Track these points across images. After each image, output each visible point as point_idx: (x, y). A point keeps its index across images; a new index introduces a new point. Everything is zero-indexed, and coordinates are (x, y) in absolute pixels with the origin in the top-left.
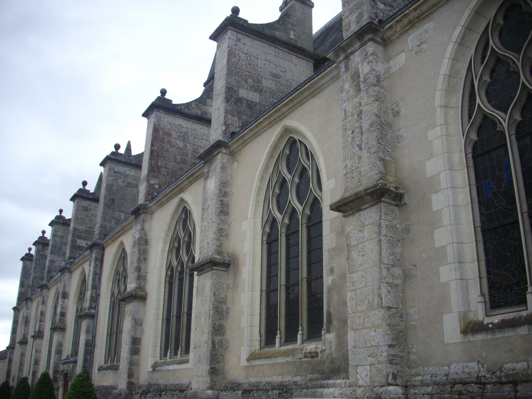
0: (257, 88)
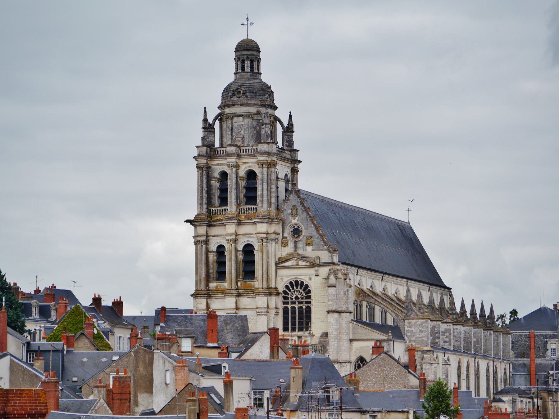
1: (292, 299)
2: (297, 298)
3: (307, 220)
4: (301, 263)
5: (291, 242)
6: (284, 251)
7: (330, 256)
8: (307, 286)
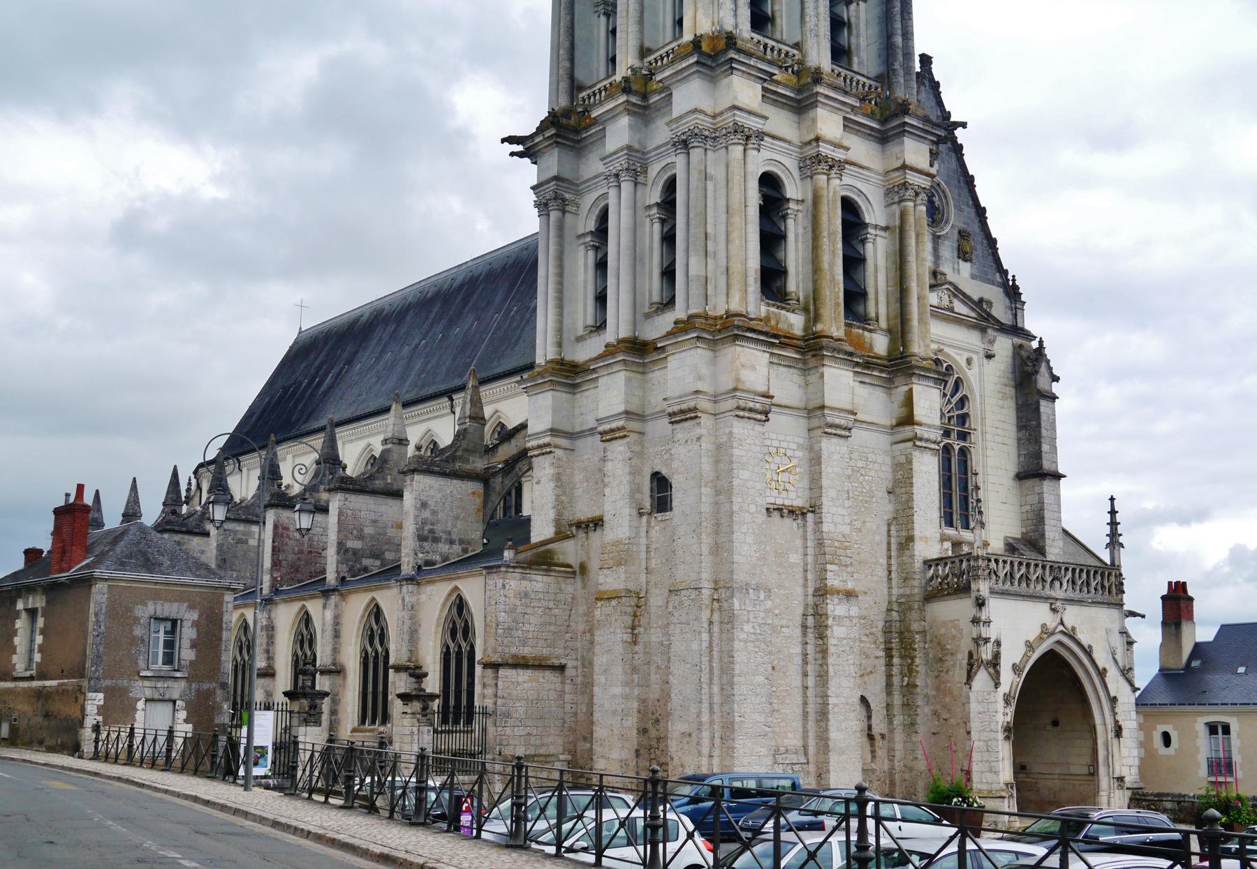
0: (361, 537)
3: (959, 182)
4: (960, 308)
8: (958, 384)
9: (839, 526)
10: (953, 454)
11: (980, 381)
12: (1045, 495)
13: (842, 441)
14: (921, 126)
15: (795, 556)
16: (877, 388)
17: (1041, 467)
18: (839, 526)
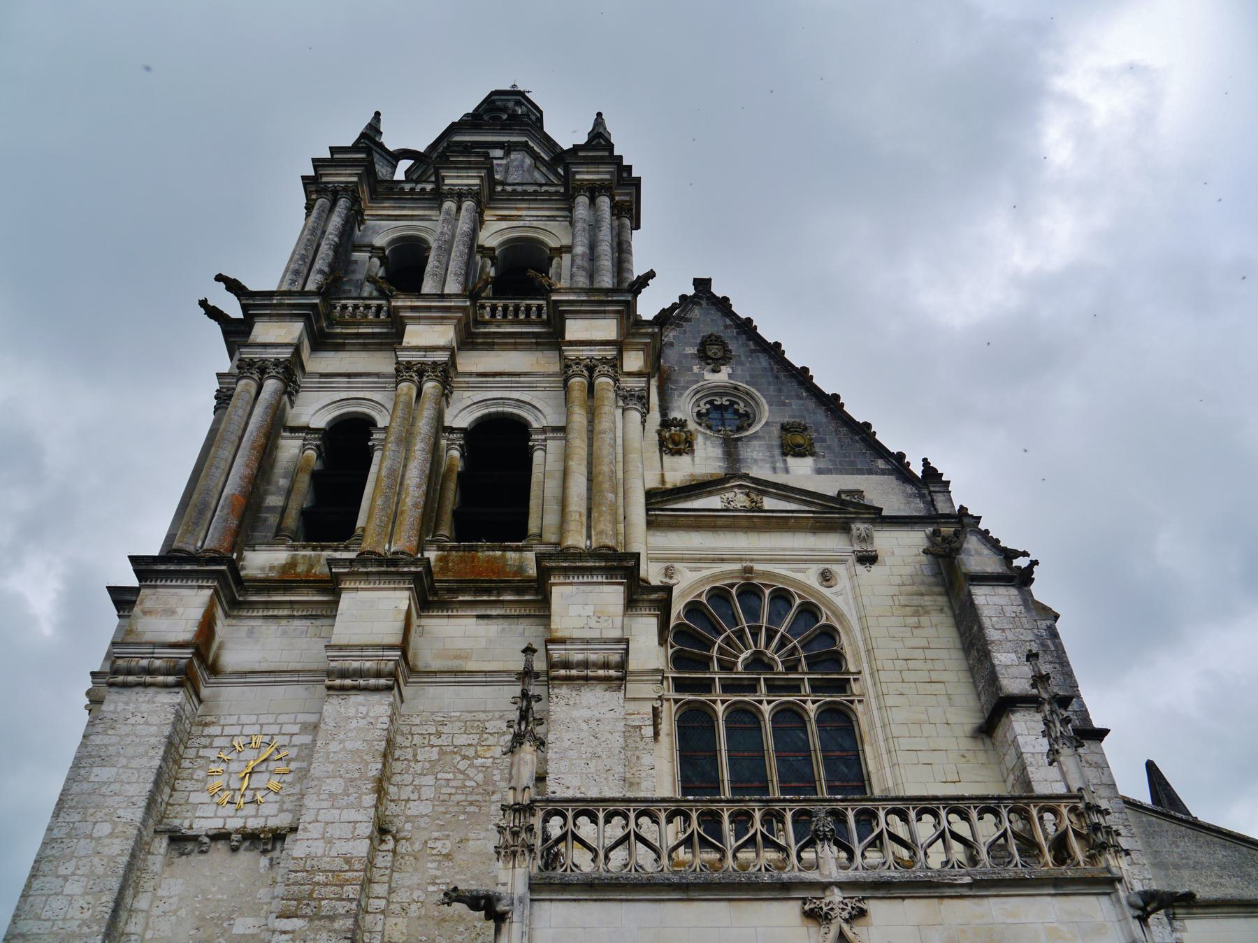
1: (726, 667)
2: (758, 662)
3: (777, 377)
5: (706, 437)
6: (673, 470)
7: (914, 495)
8: (809, 611)
9: (338, 844)
10: (807, 719)
11: (855, 598)
12: (1021, 740)
13: (376, 698)
14: (585, 298)
15: (251, 921)
16: (521, 620)
17: (999, 688)
18: (338, 844)
